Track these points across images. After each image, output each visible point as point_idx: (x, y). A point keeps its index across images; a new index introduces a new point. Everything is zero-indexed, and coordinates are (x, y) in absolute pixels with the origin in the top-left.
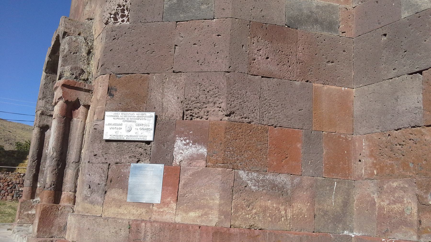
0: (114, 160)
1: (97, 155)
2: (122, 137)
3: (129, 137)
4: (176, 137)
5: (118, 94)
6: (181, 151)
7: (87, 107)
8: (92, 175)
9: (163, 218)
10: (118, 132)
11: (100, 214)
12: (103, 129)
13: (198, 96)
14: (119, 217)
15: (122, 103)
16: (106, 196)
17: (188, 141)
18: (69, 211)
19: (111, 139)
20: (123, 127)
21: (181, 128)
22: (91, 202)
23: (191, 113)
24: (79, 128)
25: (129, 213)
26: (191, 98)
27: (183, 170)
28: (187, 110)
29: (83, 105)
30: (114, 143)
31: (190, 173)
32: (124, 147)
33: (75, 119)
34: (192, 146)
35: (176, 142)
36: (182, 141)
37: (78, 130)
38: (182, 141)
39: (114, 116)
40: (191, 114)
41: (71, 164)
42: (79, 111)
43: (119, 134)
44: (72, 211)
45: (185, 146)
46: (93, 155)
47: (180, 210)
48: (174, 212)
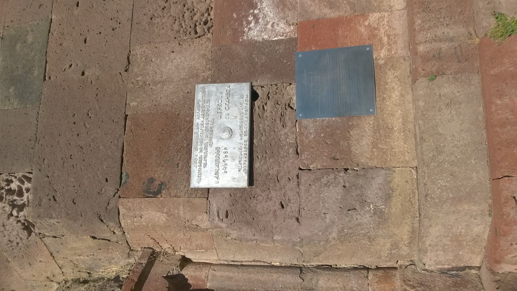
0: (291, 159)
1: (281, 202)
2: (243, 146)
4: (244, 41)
5: (159, 173)
6: (269, 26)
7: (185, 261)
8: (326, 205)
9: (400, 32)
12: (227, 195)
13: (171, 17)
14: (411, 126)
15: (177, 162)
16: (369, 164)
17: (250, 18)
18: (414, 272)
19: (247, 168)
20: (222, 144)
21: (228, 35)
22: (385, 201)
23: (200, 24)
24: (227, 273)
26: (174, 29)
27: (303, 16)
28: (196, 33)
29: (181, 270)
30: (257, 165)
34: (259, 9)
35: (252, 38)
37: (231, 275)
38: (250, 29)
39: (201, 166)
40: (202, 23)
41: (306, 283)
42: (192, 276)
43: (237, 151)
44: (413, 266)
45: (260, 21)
46: (283, 211)
47: (381, 4)
48: (386, 14)
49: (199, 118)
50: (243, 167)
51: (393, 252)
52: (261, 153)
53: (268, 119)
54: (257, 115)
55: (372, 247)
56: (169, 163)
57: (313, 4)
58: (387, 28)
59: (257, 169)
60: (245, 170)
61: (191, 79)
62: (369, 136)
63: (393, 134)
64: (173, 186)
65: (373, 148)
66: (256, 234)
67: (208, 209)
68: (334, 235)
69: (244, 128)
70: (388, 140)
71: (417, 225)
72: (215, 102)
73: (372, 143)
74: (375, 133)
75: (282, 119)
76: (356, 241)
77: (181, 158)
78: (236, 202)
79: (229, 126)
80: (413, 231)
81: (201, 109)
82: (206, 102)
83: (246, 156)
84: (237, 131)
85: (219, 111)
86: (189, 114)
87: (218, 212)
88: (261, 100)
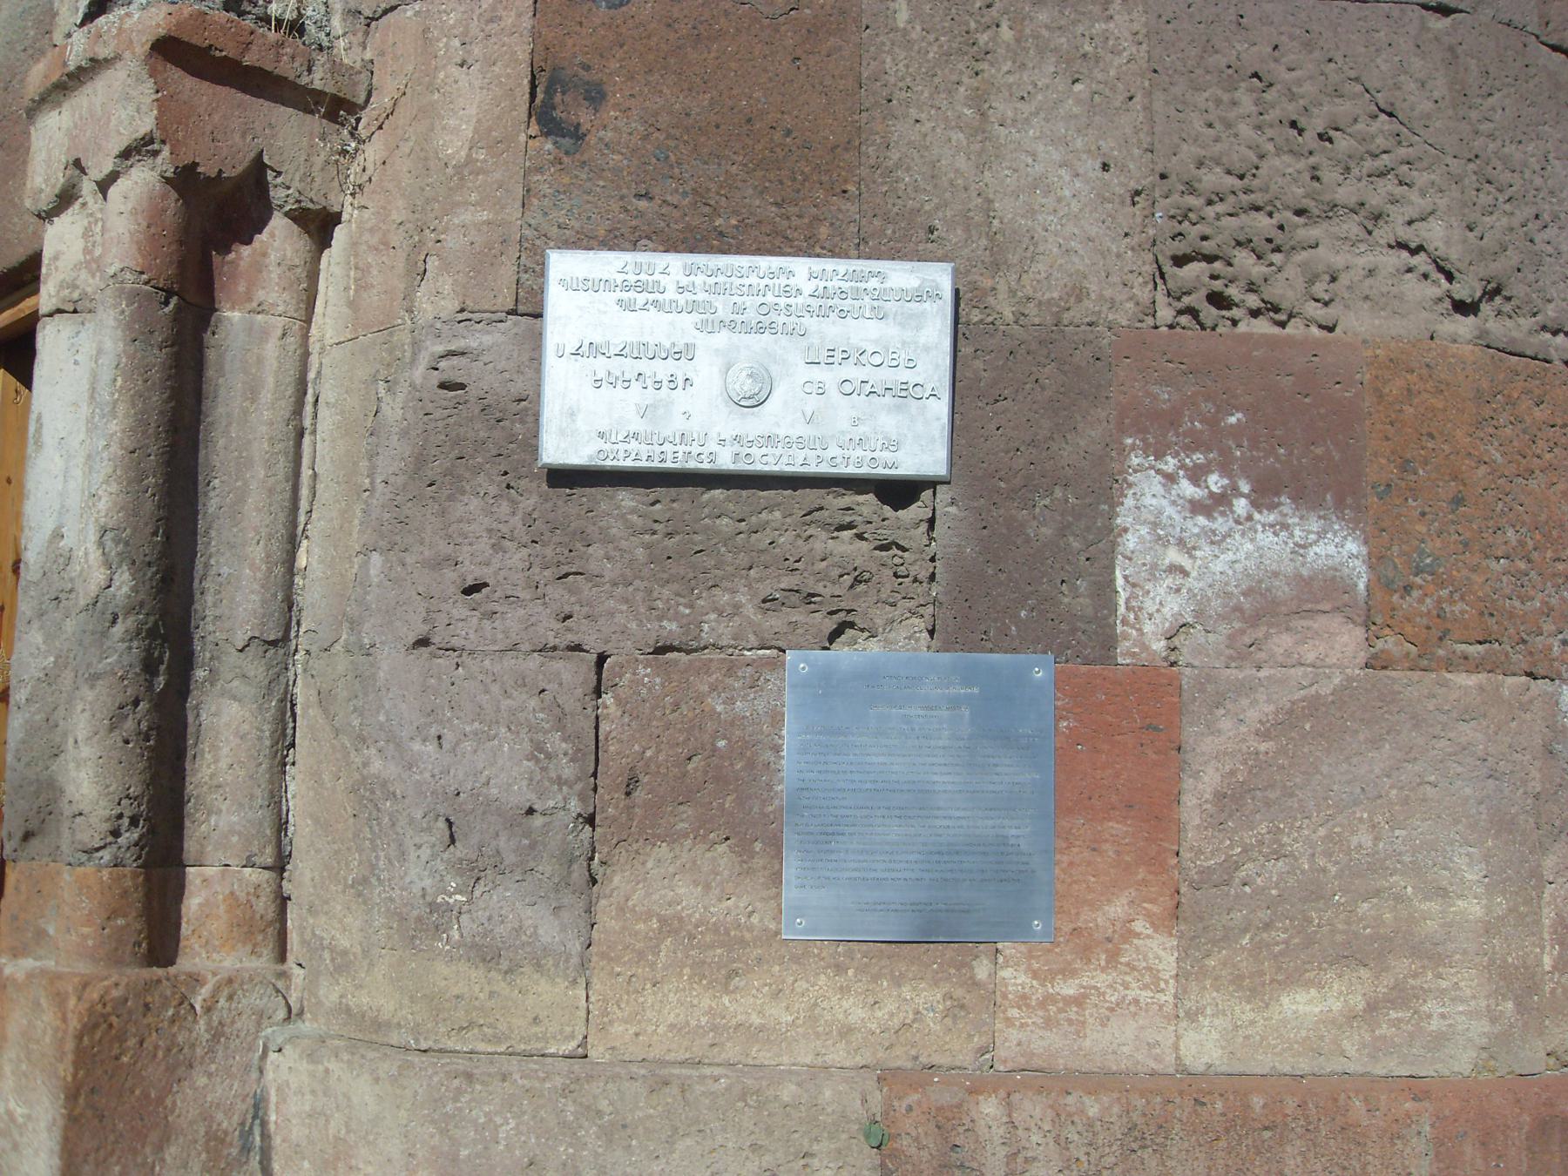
0: (640, 624)
1: (486, 585)
2: (695, 449)
3: (754, 451)
4: (1123, 452)
5: (620, 124)
6: (1173, 556)
8: (467, 746)
9: (1087, 1043)
10: (661, 411)
11: (572, 1036)
12: (518, 387)
13: (1255, 159)
14: (731, 1052)
15: (656, 191)
16: (603, 902)
17: (1215, 482)
18: (261, 1016)
19: (609, 463)
20: (705, 371)
21: (1156, 389)
22: (474, 946)
23: (1214, 277)
24: (271, 381)
25: (813, 1019)
26: (1203, 170)
27: (1202, 690)
28: (1180, 261)
29: (287, 214)
30: (627, 498)
31: (1258, 710)
32: (707, 528)
33: (232, 316)
34: (1250, 518)
35: (1130, 486)
36: (1170, 478)
37: (266, 396)
38: (1170, 478)
39: (627, 288)
40: (1217, 285)
41: (232, 658)
42: (265, 255)
43: (677, 424)
44: (281, 1014)
45: (1201, 520)
46: (453, 590)
47: (1208, 983)
48: (1167, 998)
49: (811, 277)
51: (327, 955)
52: (667, 516)
53: (800, 542)
54: (819, 501)
55: (340, 888)
56: (654, 160)
57: (1245, 730)
58: (1113, 999)
59: (612, 498)
60: (602, 457)
61: (984, 242)
62: (705, 908)
63: (707, 988)
64: (566, 180)
65: (663, 921)
66: (390, 488)
67: (476, 316)
68: (377, 765)
69: (764, 450)
70: (687, 971)
71: (394, 1038)
72: (876, 342)
73: (681, 919)
74: (716, 931)
75: (795, 598)
76: (356, 835)
77: (670, 208)
78: (493, 421)
79: (775, 394)
80: (380, 1025)
82: (876, 304)
83: (657, 459)
84: (755, 424)
85: (839, 356)
86: (842, 234)
87: (463, 354)
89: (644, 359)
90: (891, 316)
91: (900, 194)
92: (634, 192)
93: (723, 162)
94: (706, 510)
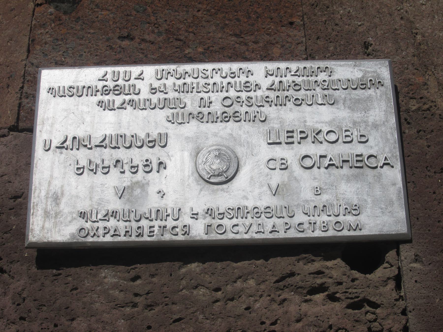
2: (170, 223)
3: (226, 222)
10: (138, 191)
19: (90, 239)
39: (106, 91)
49: (268, 74)
50: (96, 225)
52: (147, 289)
53: (275, 306)
54: (290, 268)
56: (134, 13)
60: (83, 233)
61: (411, 50)
69: (235, 221)
72: (330, 123)
77: (148, 44)
81: (301, 79)
82: (326, 92)
83: (134, 234)
85: (297, 136)
88: (345, 278)
89: (122, 149)
90: (342, 101)
91: (337, 22)
92: (118, 35)
93: (190, 10)
94: (184, 282)
